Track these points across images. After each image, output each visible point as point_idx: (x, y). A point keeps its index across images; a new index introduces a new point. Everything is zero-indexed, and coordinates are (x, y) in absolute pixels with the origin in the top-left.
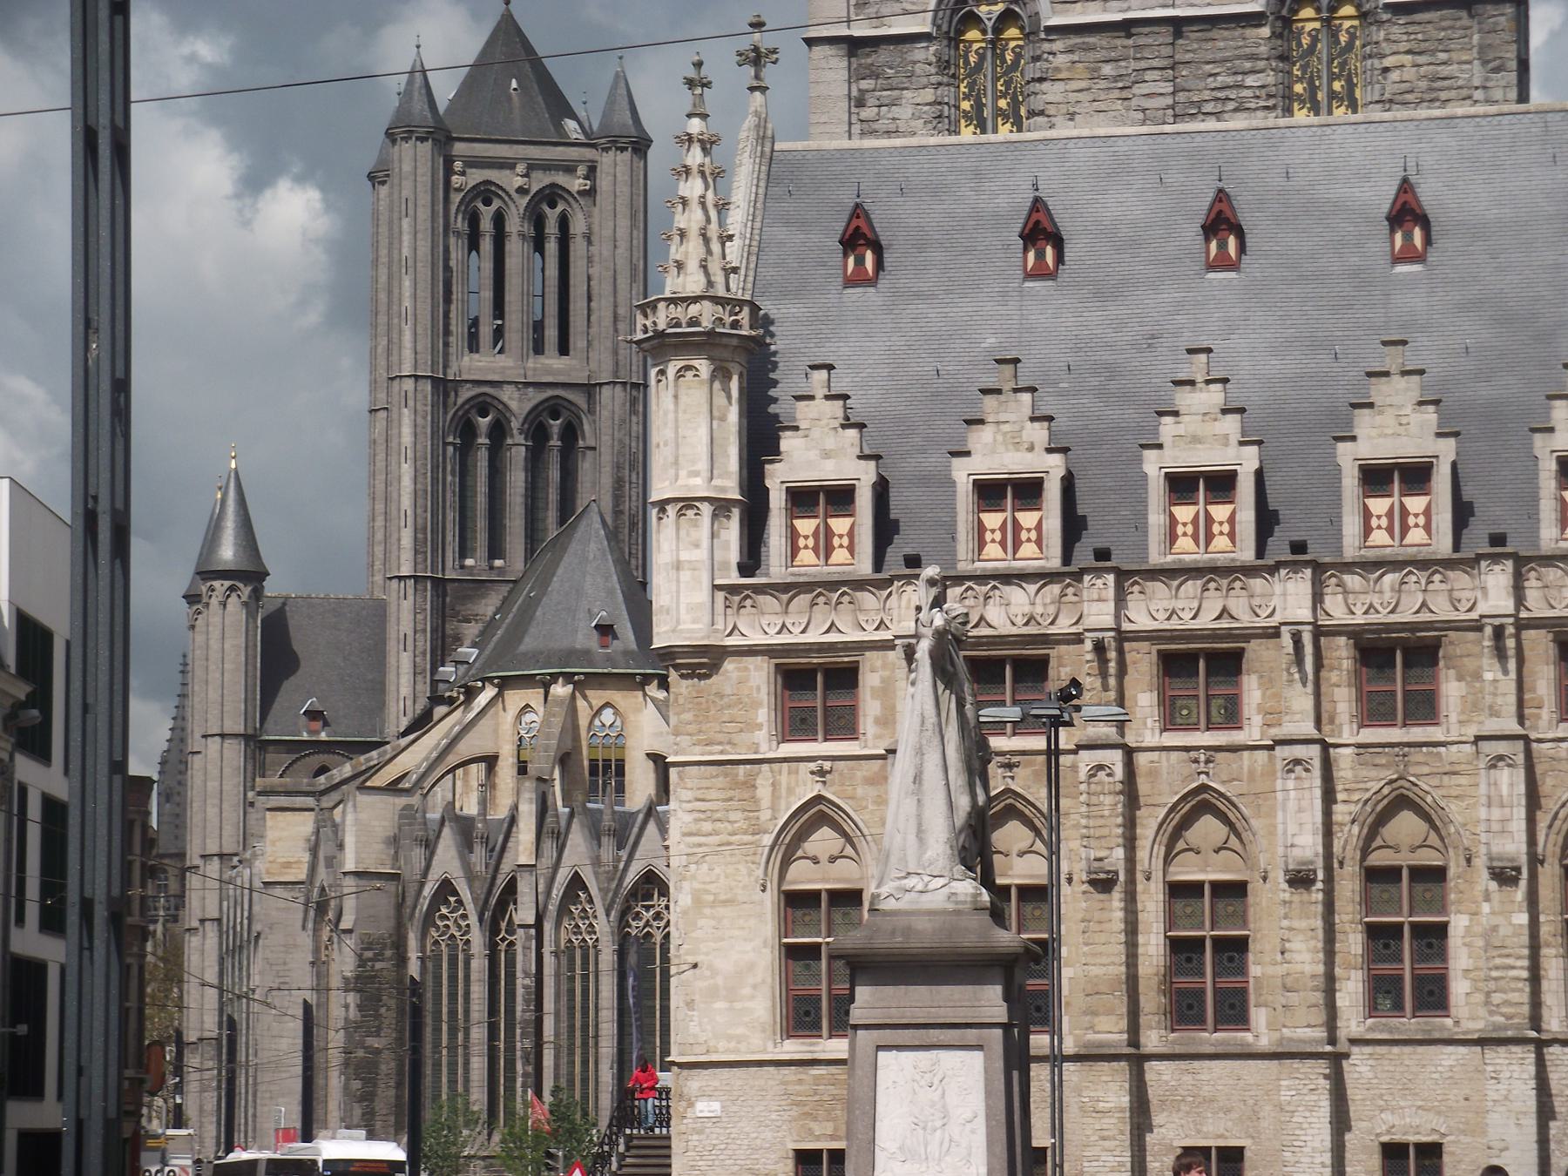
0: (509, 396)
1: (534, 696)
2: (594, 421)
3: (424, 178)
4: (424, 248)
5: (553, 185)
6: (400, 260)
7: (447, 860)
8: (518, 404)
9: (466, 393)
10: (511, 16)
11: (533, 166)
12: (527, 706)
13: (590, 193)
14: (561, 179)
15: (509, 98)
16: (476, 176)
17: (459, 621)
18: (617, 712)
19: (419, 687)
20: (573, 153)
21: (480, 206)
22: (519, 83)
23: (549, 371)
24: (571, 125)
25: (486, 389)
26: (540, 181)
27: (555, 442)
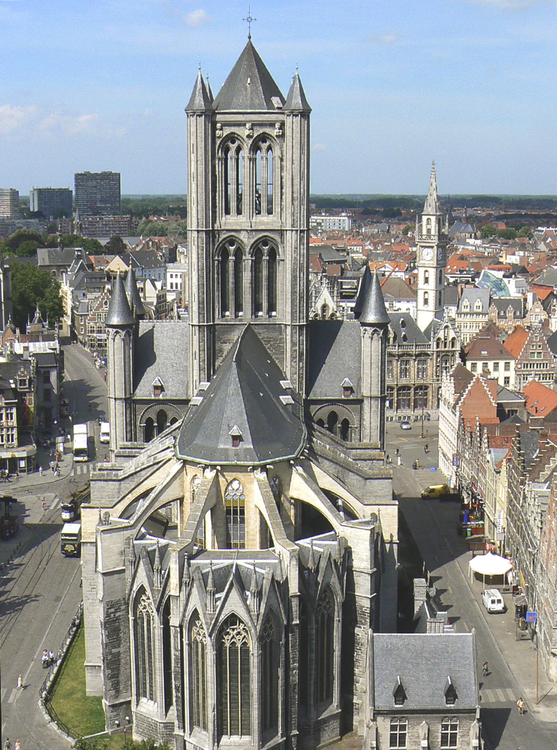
0: (243, 237)
1: (198, 471)
2: (284, 247)
3: (201, 135)
4: (201, 168)
5: (264, 133)
6: (191, 174)
7: (142, 578)
8: (247, 240)
9: (223, 236)
10: (252, 45)
11: (254, 125)
12: (196, 475)
13: (282, 136)
14: (268, 130)
15: (246, 89)
16: (227, 131)
17: (221, 343)
18: (239, 483)
19: (202, 376)
20: (273, 117)
21: (231, 145)
22: (251, 81)
23: (263, 223)
24: (276, 101)
25: (233, 234)
26: (258, 131)
27: (265, 258)
